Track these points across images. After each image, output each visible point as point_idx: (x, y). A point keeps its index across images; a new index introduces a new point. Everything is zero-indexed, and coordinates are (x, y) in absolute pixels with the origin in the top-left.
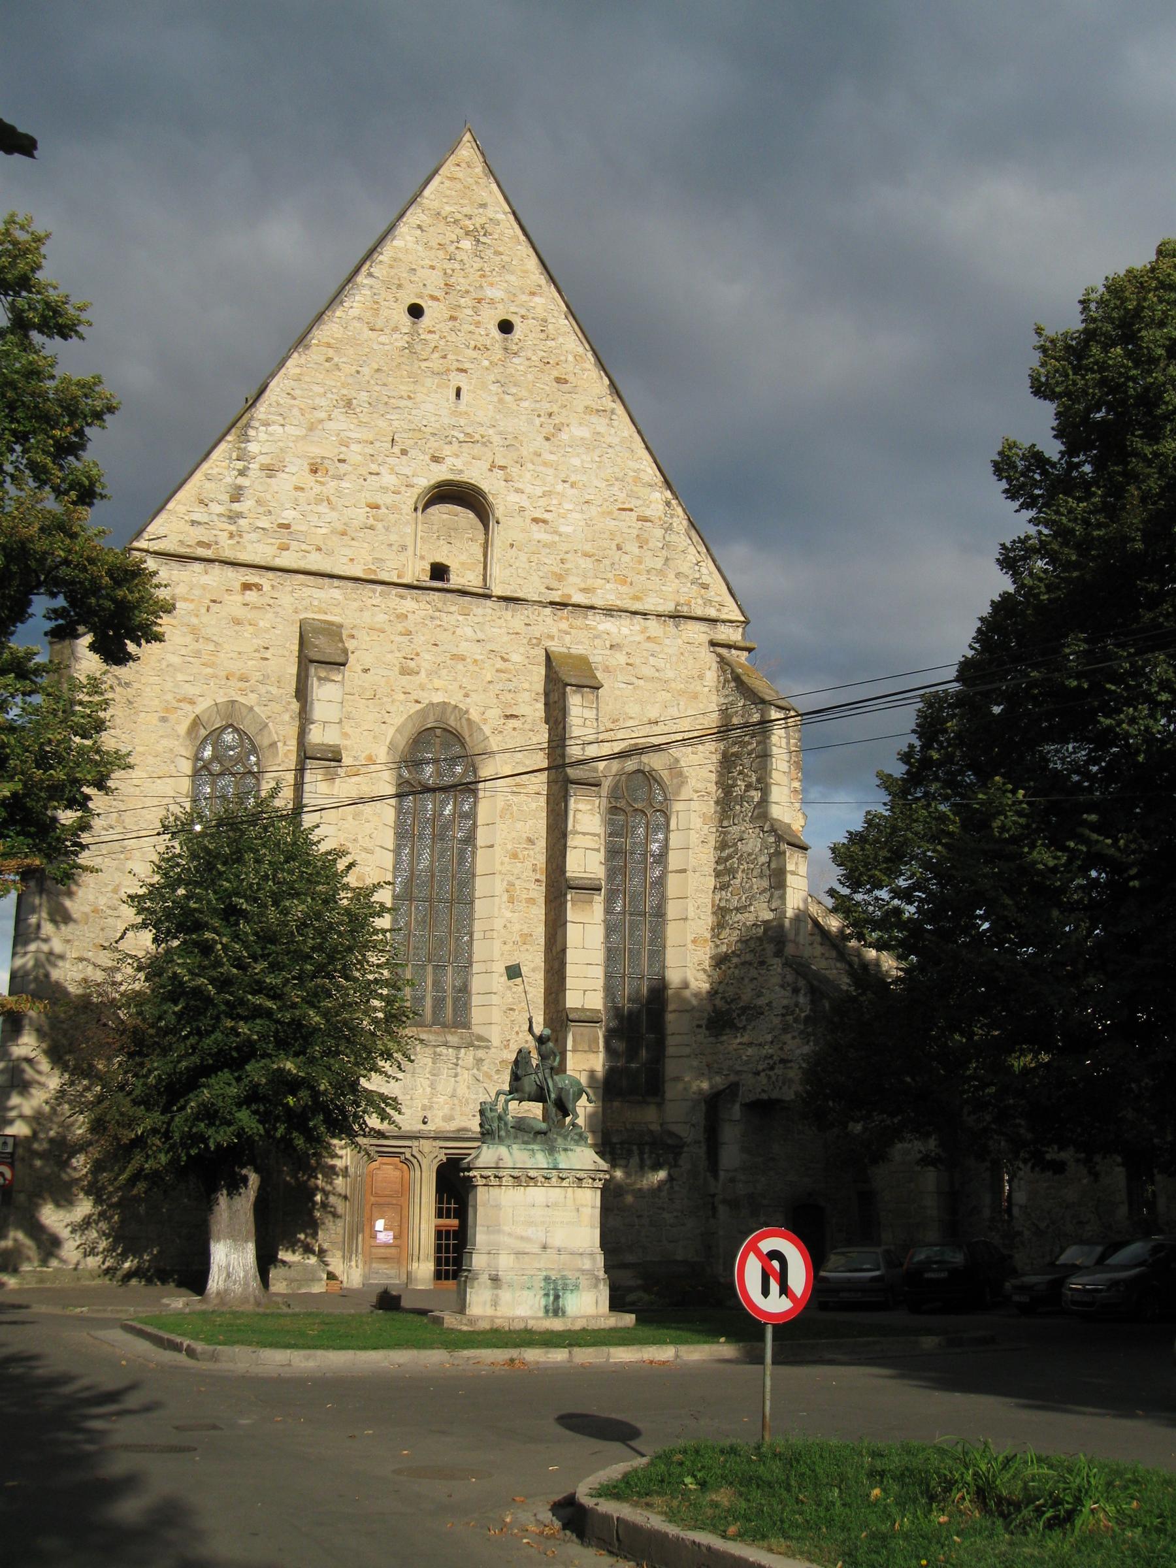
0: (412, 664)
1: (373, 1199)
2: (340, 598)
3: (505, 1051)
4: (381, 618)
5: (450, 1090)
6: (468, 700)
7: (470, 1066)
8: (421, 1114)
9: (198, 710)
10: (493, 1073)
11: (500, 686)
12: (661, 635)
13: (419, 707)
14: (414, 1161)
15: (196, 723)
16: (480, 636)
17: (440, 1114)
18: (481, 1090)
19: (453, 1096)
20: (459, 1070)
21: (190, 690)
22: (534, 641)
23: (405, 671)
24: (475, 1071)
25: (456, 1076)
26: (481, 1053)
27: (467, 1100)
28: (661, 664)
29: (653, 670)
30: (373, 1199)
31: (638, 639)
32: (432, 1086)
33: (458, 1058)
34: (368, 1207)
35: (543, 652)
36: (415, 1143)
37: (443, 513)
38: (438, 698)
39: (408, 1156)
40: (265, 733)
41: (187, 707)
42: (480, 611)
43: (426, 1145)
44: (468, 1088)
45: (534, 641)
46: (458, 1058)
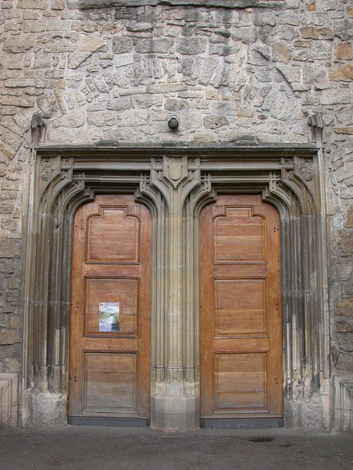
1: (87, 268)
3: (309, 14)
5: (216, 77)
7: (250, 35)
8: (165, 115)
10: (290, 45)
17: (201, 115)
18: (273, 74)
19: (222, 86)
20: (231, 43)
24: (259, 44)
25: (227, 52)
26: (267, 17)
27: (248, 92)
30: (87, 268)
32: (185, 70)
33: (228, 26)
34: (77, 282)
36: (152, 166)
39: (144, 188)
44: (250, 71)
46: (228, 26)
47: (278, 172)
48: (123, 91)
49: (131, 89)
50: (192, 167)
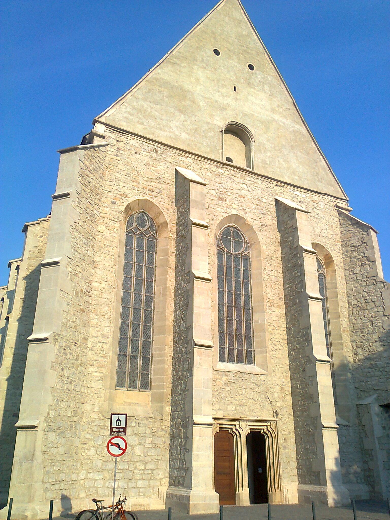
0: (223, 196)
2: (192, 162)
4: (209, 174)
6: (247, 215)
9: (131, 200)
11: (259, 211)
12: (317, 200)
13: (227, 215)
14: (237, 433)
15: (128, 208)
16: (250, 189)
21: (126, 191)
22: (271, 195)
23: (221, 199)
28: (318, 211)
29: (315, 213)
31: (309, 200)
35: (274, 199)
37: (229, 137)
38: (234, 212)
40: (161, 217)
41: (125, 199)
42: (249, 179)
43: (243, 424)
45: (271, 195)
47: (267, 426)
48: (228, 399)
49: (230, 399)
50: (246, 424)
